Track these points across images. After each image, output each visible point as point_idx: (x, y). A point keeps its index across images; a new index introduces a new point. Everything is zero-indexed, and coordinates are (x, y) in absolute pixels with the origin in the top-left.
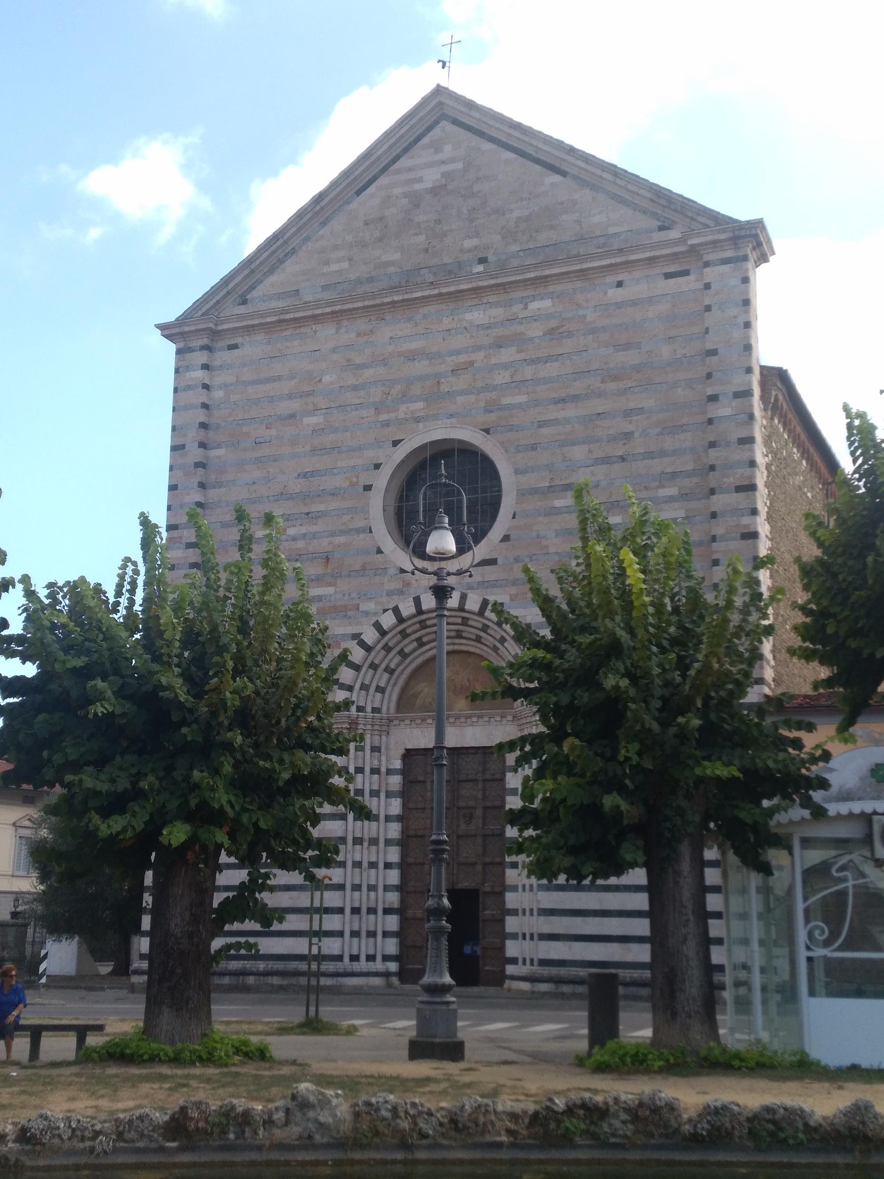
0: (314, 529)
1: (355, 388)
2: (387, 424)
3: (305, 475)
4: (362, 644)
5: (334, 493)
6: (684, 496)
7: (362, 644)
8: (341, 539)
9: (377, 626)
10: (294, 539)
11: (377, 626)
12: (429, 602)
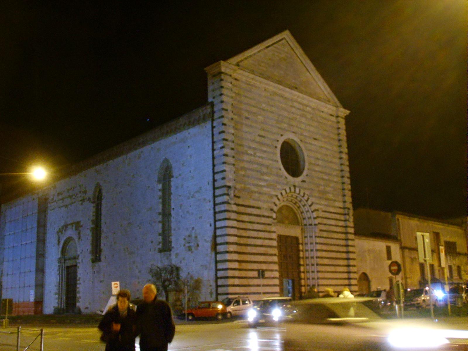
0: (264, 156)
1: (271, 112)
2: (279, 128)
3: (260, 136)
4: (279, 199)
5: (268, 145)
6: (337, 176)
7: (279, 199)
8: (271, 162)
9: (281, 194)
10: (259, 157)
11: (281, 194)
12: (293, 190)
